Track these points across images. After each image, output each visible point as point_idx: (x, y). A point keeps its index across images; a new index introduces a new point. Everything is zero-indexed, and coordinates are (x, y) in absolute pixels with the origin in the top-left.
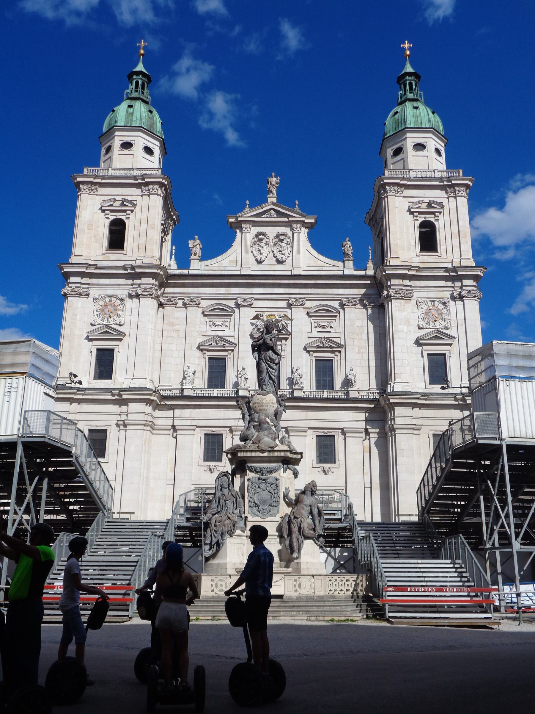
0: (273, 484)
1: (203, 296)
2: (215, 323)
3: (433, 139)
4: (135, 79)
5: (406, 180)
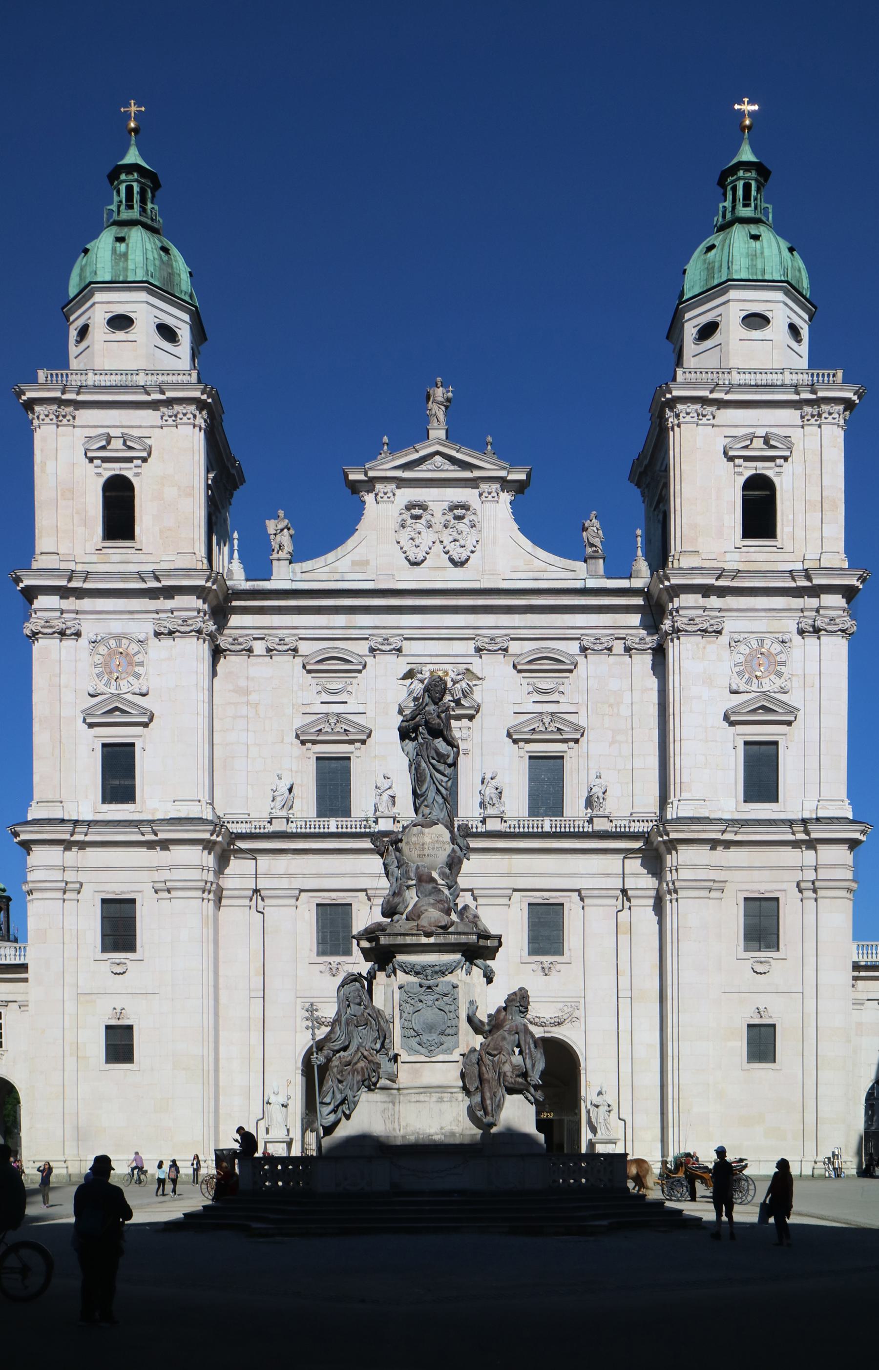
1: (303, 633)
2: (329, 686)
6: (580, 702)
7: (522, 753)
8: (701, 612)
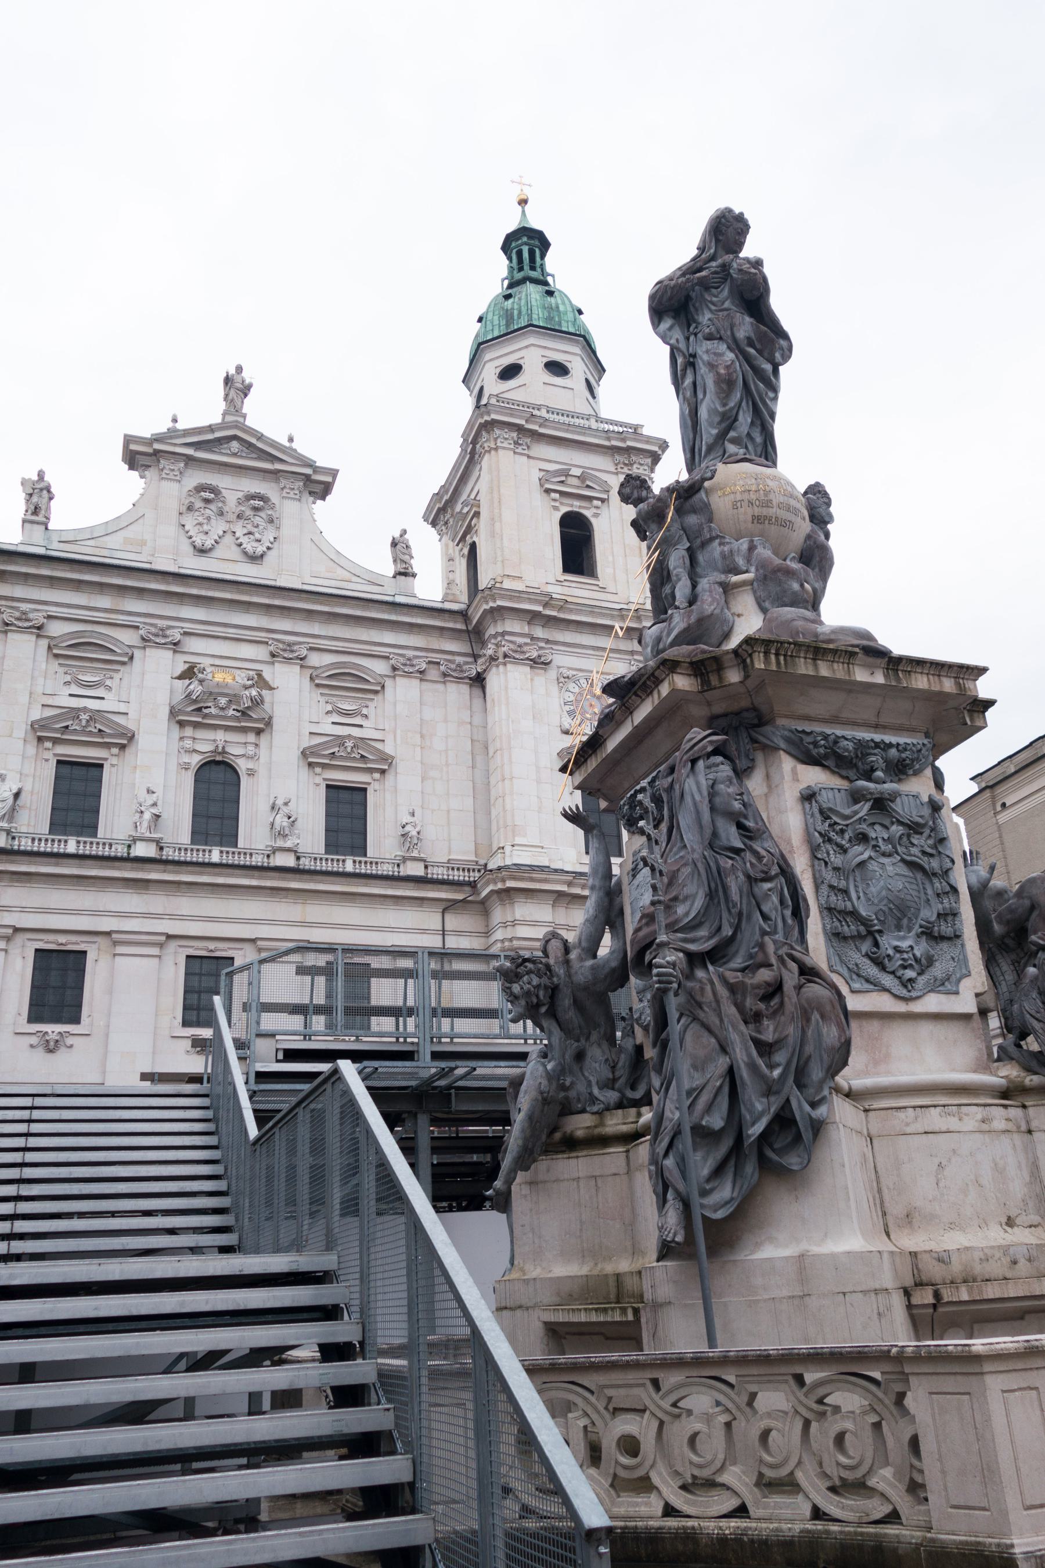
0: (914, 828)
1: (53, 610)
2: (80, 677)
5: (535, 423)
6: (387, 728)
7: (318, 780)
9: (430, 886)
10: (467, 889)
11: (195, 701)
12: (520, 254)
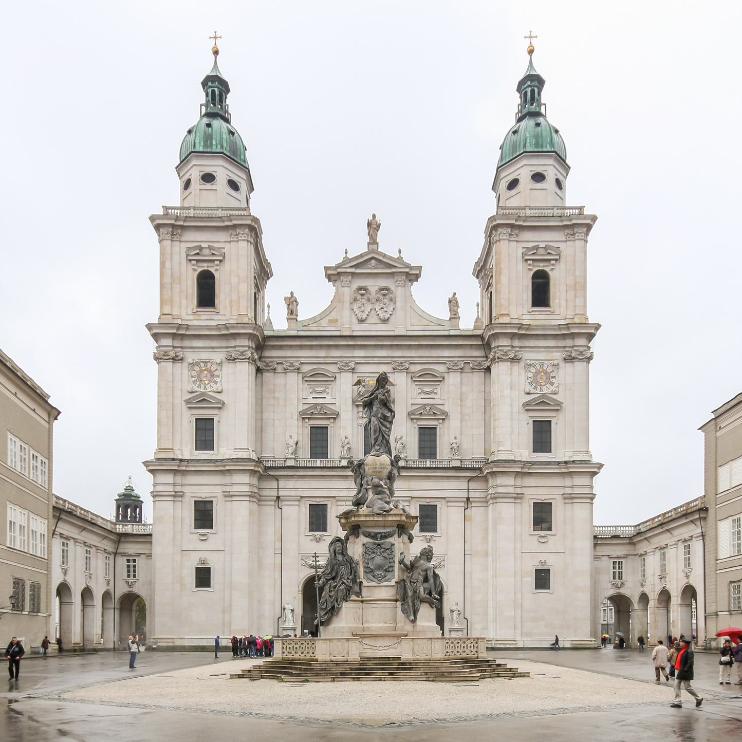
3: (555, 167)
4: (211, 87)
8: (510, 348)
9: (462, 471)
10: (478, 471)
11: (362, 395)
12: (526, 94)
